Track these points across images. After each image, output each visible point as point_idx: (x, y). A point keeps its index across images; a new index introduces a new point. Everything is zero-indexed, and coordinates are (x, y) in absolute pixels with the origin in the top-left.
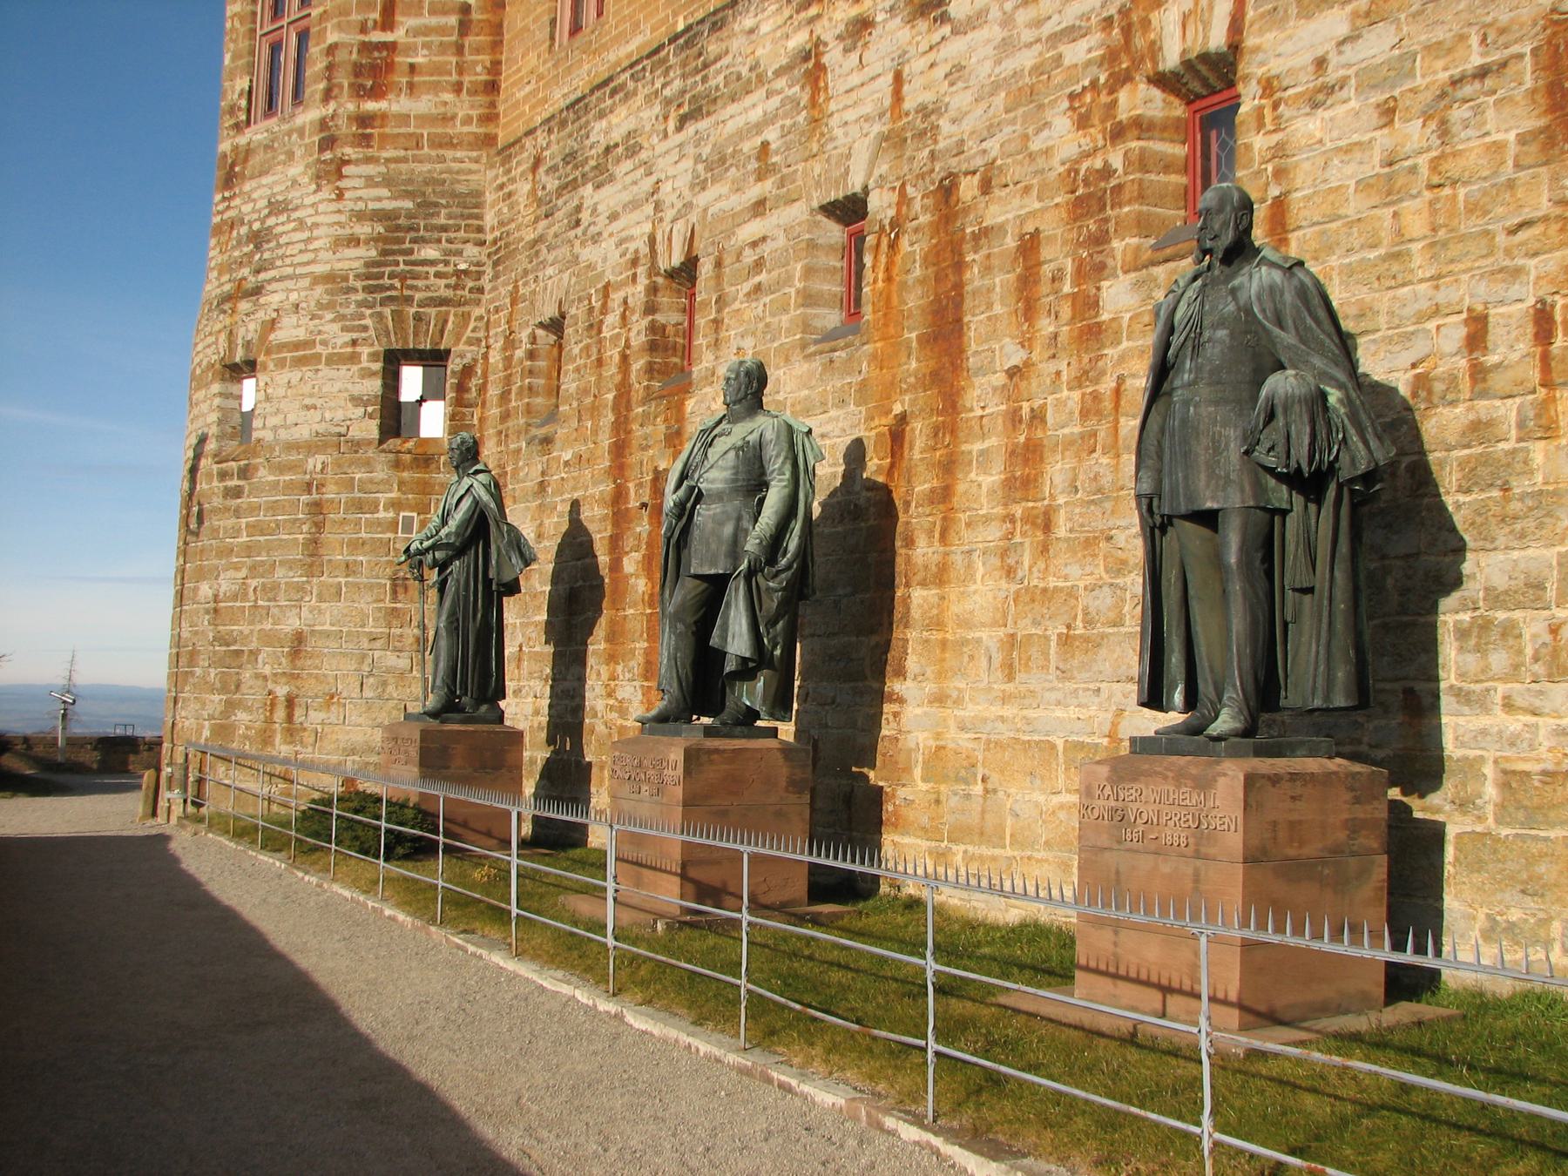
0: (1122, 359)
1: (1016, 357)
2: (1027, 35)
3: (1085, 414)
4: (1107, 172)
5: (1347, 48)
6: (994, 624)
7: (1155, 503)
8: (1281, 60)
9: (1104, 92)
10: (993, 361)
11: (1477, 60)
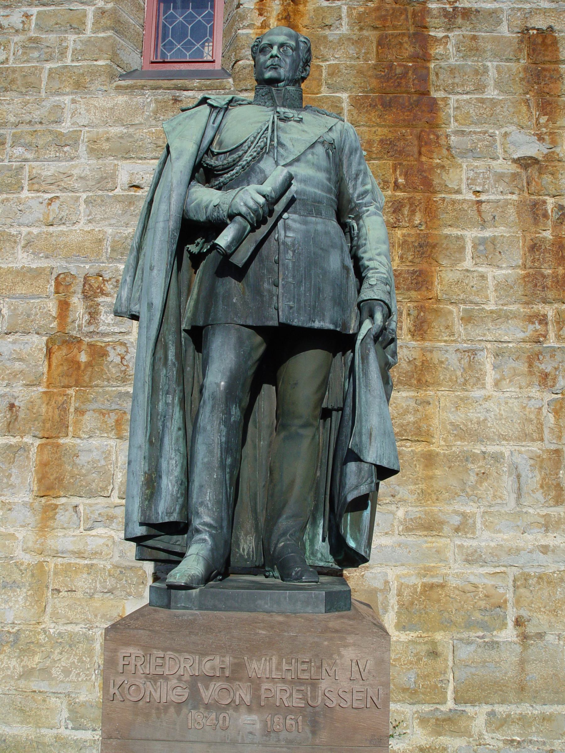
6: (526, 436)
10: (492, 144)
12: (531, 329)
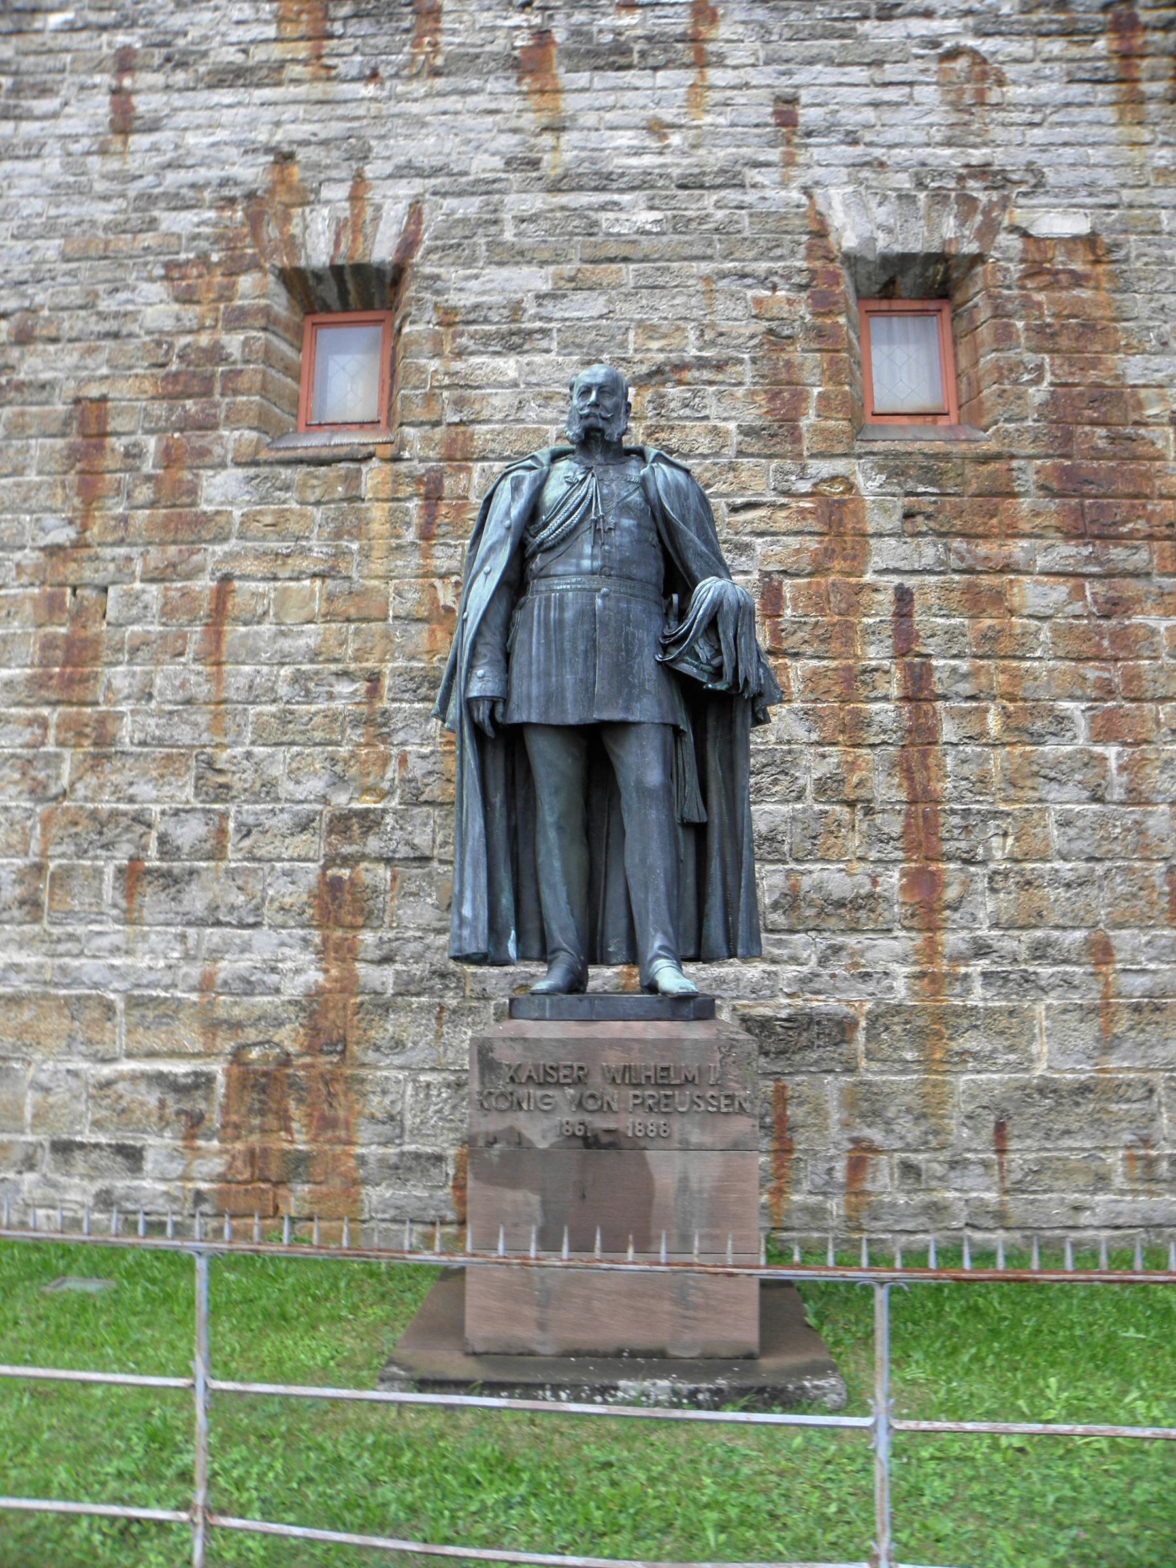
0: (231, 556)
1: (63, 535)
2: (100, 187)
3: (168, 611)
4: (216, 354)
5: (549, 304)
7: (500, 708)
8: (462, 295)
9: (219, 271)
11: (694, 352)
12: (27, 735)
